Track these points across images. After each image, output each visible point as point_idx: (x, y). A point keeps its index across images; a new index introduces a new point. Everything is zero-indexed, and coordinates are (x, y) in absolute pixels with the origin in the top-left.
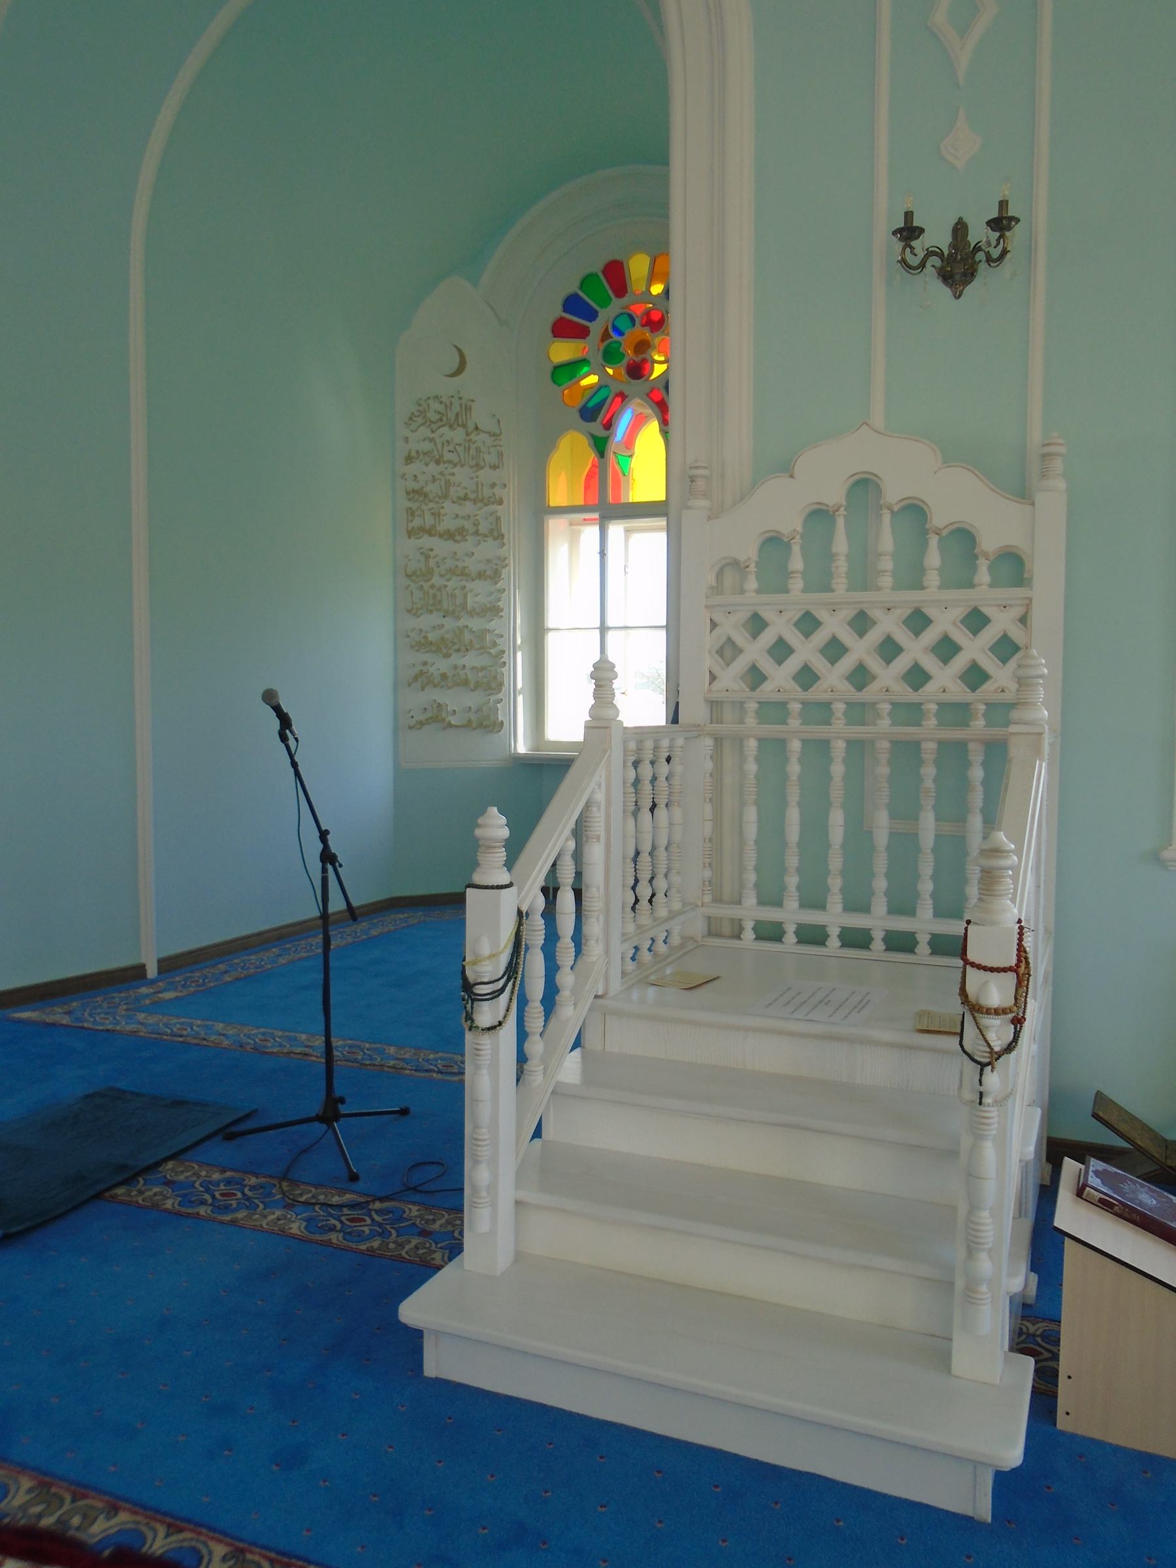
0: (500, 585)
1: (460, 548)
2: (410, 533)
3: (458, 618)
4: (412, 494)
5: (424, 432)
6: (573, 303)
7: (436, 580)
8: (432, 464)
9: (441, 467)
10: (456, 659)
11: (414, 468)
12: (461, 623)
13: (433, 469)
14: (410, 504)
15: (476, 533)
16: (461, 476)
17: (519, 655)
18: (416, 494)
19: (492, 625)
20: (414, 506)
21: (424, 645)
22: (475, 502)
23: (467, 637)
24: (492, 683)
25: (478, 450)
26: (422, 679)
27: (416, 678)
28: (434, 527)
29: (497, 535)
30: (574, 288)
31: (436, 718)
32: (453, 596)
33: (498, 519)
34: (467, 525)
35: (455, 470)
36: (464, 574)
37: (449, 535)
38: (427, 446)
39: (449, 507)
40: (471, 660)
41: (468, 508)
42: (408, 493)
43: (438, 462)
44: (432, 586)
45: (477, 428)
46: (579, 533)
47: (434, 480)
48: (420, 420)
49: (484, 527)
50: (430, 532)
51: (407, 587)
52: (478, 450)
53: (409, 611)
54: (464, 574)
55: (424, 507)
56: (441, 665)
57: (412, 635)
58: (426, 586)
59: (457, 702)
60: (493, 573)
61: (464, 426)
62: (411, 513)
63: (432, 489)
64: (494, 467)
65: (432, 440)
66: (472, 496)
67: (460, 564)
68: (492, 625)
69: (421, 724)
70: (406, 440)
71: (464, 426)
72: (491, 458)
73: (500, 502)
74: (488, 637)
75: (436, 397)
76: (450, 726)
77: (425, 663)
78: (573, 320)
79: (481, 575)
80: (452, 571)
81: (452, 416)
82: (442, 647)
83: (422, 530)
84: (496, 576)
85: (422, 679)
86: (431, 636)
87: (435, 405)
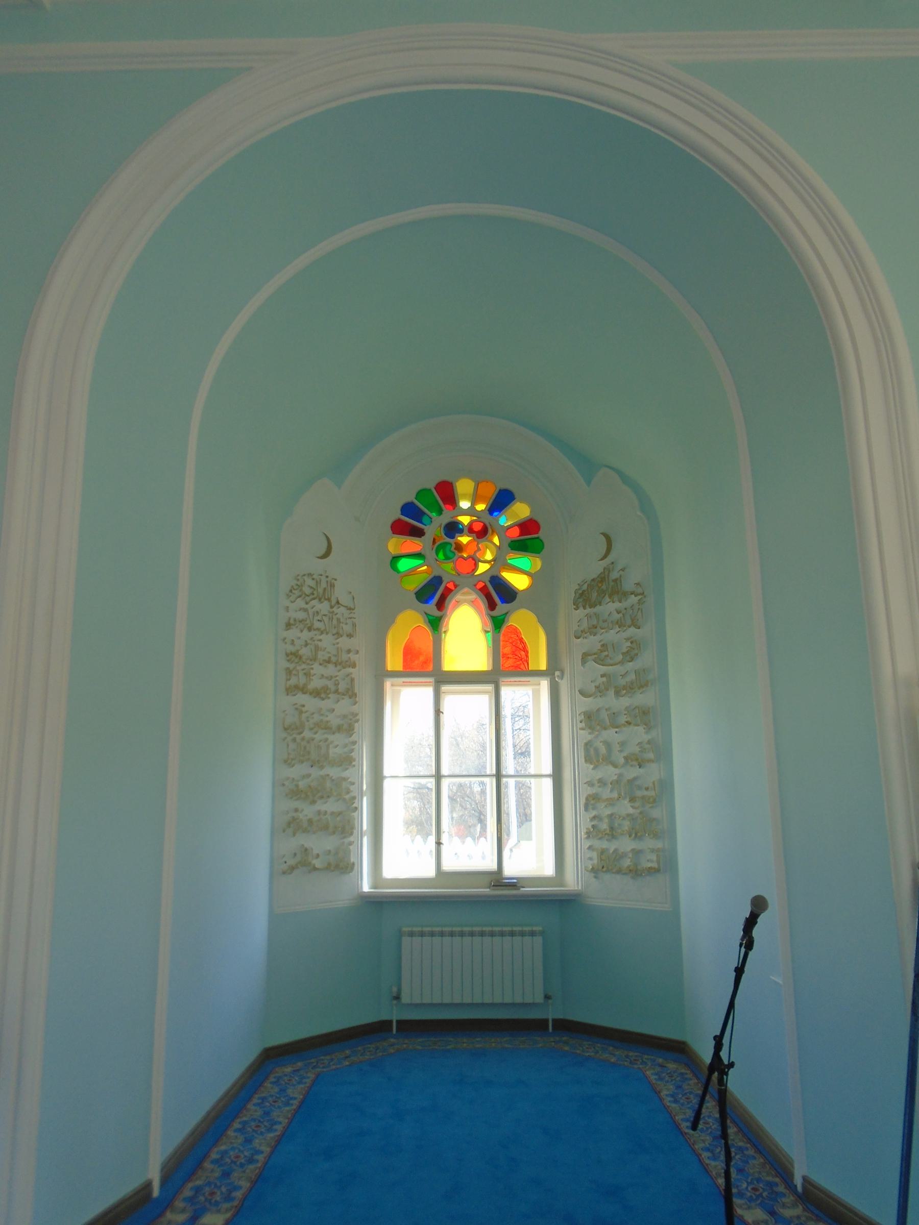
0: (354, 737)
1: (325, 704)
2: (291, 690)
3: (322, 767)
4: (294, 656)
5: (300, 603)
6: (409, 509)
7: (307, 734)
8: (305, 632)
9: (313, 633)
10: (321, 806)
11: (293, 633)
12: (323, 772)
13: (306, 635)
14: (288, 665)
15: (336, 691)
16: (327, 641)
17: (365, 799)
18: (294, 656)
19: (346, 774)
20: (291, 666)
21: (296, 793)
22: (336, 664)
23: (328, 784)
24: (344, 827)
25: (338, 620)
26: (294, 825)
27: (289, 824)
28: (305, 685)
29: (350, 693)
30: (410, 497)
31: (302, 863)
32: (319, 747)
33: (352, 680)
34: (330, 684)
35: (321, 637)
36: (327, 728)
37: (317, 693)
38: (301, 615)
39: (317, 669)
40: (330, 806)
41: (330, 670)
42: (287, 655)
43: (310, 629)
44: (303, 739)
45: (338, 602)
46: (399, 692)
47: (306, 645)
48: (297, 593)
49: (342, 687)
50: (303, 690)
51: (284, 739)
52: (338, 620)
53: (285, 761)
54: (327, 728)
55: (298, 668)
56: (308, 811)
57: (287, 783)
58: (298, 737)
59: (320, 844)
60: (348, 727)
61: (329, 600)
62: (289, 672)
63: (304, 652)
64: (350, 636)
65: (305, 610)
66: (334, 659)
67: (325, 719)
68: (346, 774)
69: (293, 868)
70: (287, 609)
71: (329, 600)
72: (347, 628)
73: (354, 666)
74: (344, 784)
75: (310, 575)
76: (315, 869)
77: (296, 810)
78: (408, 524)
79: (339, 729)
80: (317, 725)
81: (320, 590)
82: (313, 794)
83: (296, 687)
84: (350, 730)
85: (294, 825)
86: (302, 784)
87: (309, 582)
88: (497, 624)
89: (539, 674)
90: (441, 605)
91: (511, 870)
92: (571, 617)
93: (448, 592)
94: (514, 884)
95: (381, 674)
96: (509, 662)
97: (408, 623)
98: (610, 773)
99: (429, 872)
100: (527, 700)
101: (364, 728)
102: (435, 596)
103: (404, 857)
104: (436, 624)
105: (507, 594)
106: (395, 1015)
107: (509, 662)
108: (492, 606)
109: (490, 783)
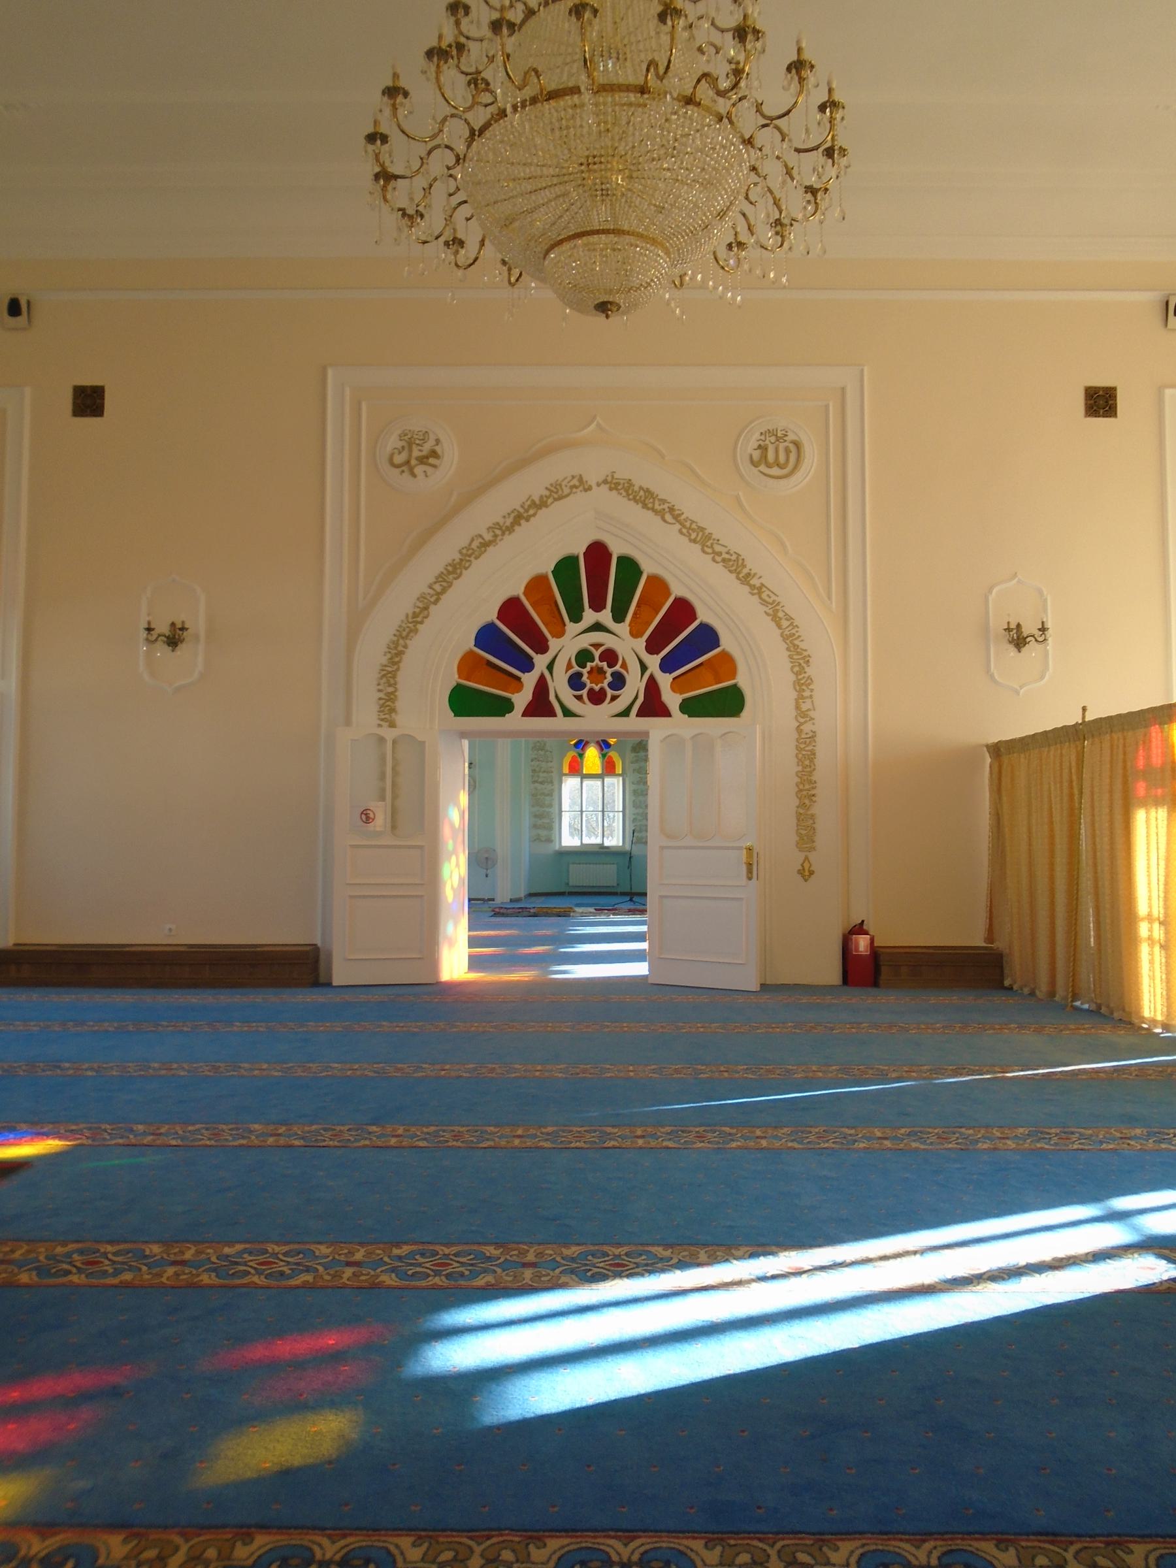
16: (543, 765)
18: (534, 771)
21: (536, 816)
24: (549, 827)
29: (552, 782)
37: (541, 783)
39: (541, 775)
54: (543, 794)
56: (540, 822)
59: (543, 833)
60: (550, 794)
85: (535, 826)
88: (604, 756)
89: (619, 775)
90: (583, 749)
91: (607, 843)
92: (630, 756)
93: (587, 743)
94: (608, 848)
95: (562, 774)
96: (609, 768)
97: (572, 753)
98: (640, 811)
99: (578, 844)
100: (615, 785)
101: (556, 794)
102: (581, 745)
103: (569, 840)
104: (581, 755)
105: (608, 745)
106: (568, 890)
107: (609, 768)
108: (602, 750)
109: (600, 814)
